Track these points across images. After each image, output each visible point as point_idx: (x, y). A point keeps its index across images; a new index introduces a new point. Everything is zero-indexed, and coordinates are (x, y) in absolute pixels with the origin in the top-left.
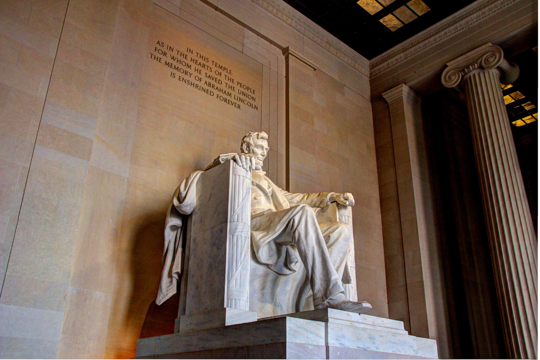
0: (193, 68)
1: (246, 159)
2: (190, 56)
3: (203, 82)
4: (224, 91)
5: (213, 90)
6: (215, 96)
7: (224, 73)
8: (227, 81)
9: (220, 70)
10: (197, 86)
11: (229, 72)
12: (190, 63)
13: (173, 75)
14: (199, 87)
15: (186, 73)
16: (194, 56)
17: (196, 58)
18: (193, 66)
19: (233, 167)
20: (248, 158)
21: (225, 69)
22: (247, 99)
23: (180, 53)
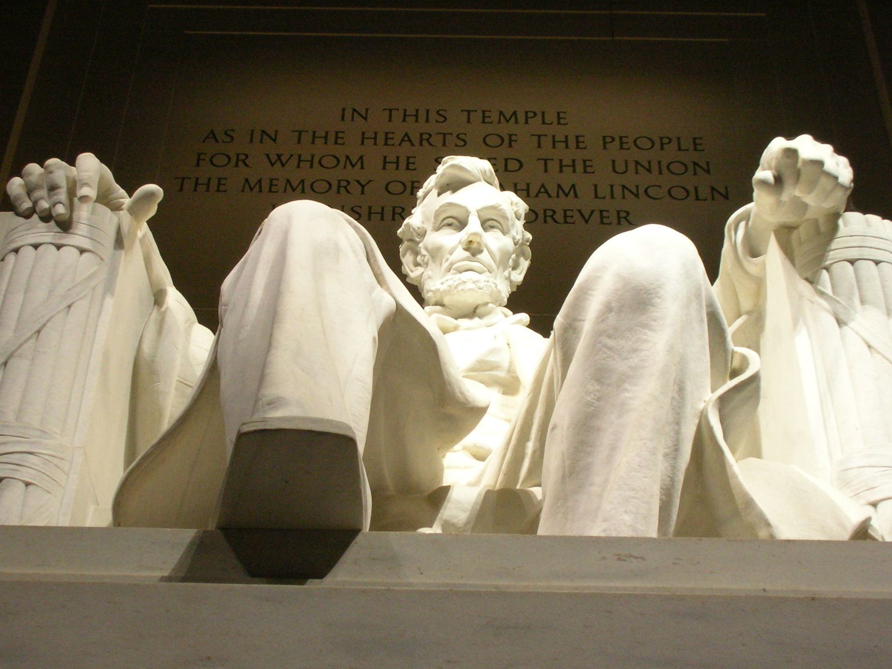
9: (505, 129)
11: (551, 117)
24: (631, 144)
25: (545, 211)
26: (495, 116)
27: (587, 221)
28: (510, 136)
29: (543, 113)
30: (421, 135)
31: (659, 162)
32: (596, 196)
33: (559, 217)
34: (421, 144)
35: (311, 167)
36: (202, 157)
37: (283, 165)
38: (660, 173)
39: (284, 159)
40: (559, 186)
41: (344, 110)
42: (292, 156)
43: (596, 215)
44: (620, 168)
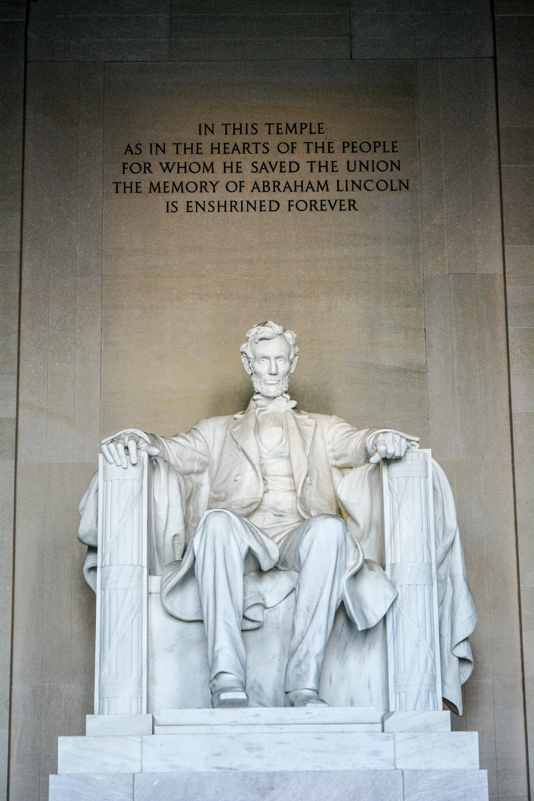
0: (218, 167)
1: (116, 448)
2: (207, 140)
3: (248, 186)
4: (305, 186)
5: (278, 196)
6: (284, 205)
7: (300, 139)
8: (312, 156)
9: (290, 138)
10: (233, 206)
11: (315, 129)
12: (208, 159)
13: (172, 207)
14: (239, 207)
15: (203, 187)
16: (219, 137)
17: (223, 139)
18: (219, 160)
19: (104, 469)
20: (120, 447)
21: (303, 126)
22: (376, 176)
23: (181, 148)
24: (358, 148)
25: (311, 201)
26: (284, 126)
27: (333, 208)
28: (292, 143)
29: (311, 124)
30: (244, 144)
31: (373, 162)
32: (338, 190)
33: (318, 206)
34: (244, 153)
35: (185, 172)
36: (126, 166)
37: (170, 171)
38: (373, 171)
39: (170, 166)
40: (319, 183)
41: (200, 125)
42: (174, 163)
43: (338, 202)
44: (352, 168)
